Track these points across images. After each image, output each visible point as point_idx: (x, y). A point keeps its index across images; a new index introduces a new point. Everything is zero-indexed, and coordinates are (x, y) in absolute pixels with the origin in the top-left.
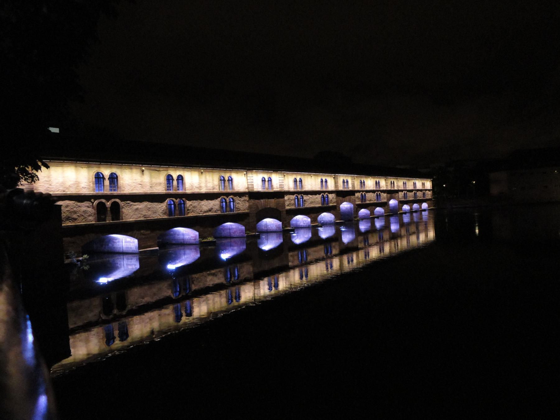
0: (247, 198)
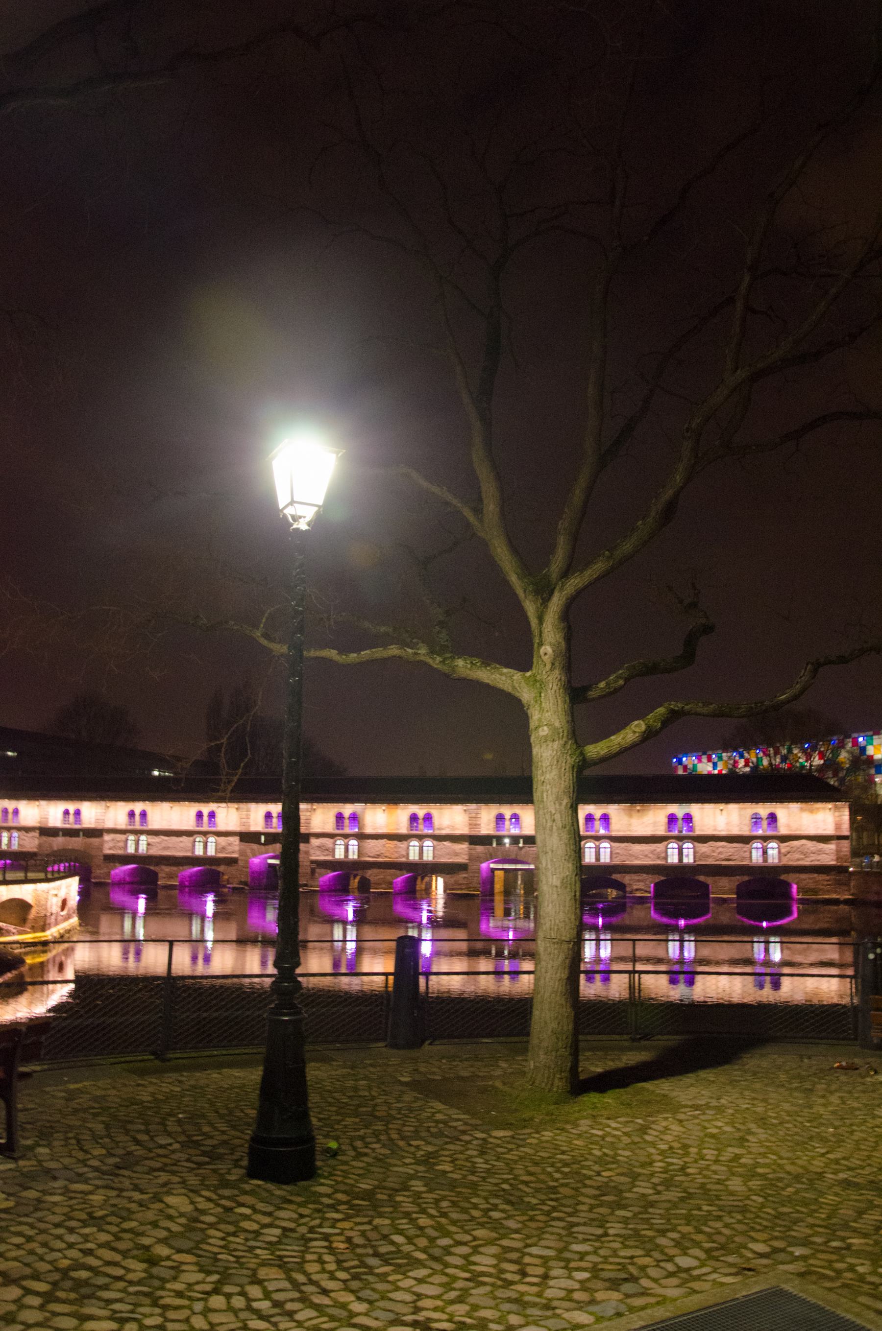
0: (36, 834)
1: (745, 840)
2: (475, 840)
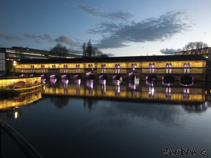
0: (48, 70)
1: (183, 68)
2: (128, 69)
